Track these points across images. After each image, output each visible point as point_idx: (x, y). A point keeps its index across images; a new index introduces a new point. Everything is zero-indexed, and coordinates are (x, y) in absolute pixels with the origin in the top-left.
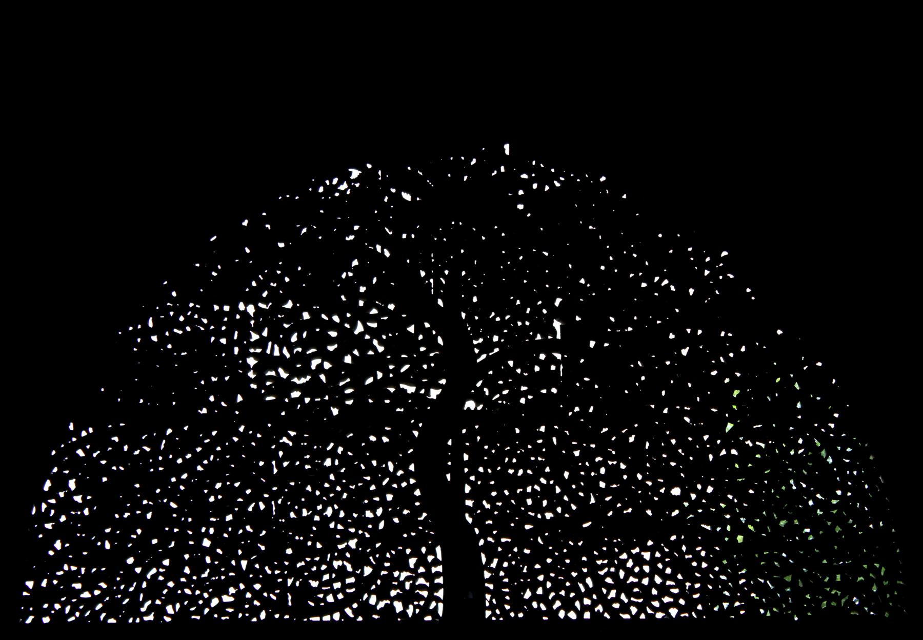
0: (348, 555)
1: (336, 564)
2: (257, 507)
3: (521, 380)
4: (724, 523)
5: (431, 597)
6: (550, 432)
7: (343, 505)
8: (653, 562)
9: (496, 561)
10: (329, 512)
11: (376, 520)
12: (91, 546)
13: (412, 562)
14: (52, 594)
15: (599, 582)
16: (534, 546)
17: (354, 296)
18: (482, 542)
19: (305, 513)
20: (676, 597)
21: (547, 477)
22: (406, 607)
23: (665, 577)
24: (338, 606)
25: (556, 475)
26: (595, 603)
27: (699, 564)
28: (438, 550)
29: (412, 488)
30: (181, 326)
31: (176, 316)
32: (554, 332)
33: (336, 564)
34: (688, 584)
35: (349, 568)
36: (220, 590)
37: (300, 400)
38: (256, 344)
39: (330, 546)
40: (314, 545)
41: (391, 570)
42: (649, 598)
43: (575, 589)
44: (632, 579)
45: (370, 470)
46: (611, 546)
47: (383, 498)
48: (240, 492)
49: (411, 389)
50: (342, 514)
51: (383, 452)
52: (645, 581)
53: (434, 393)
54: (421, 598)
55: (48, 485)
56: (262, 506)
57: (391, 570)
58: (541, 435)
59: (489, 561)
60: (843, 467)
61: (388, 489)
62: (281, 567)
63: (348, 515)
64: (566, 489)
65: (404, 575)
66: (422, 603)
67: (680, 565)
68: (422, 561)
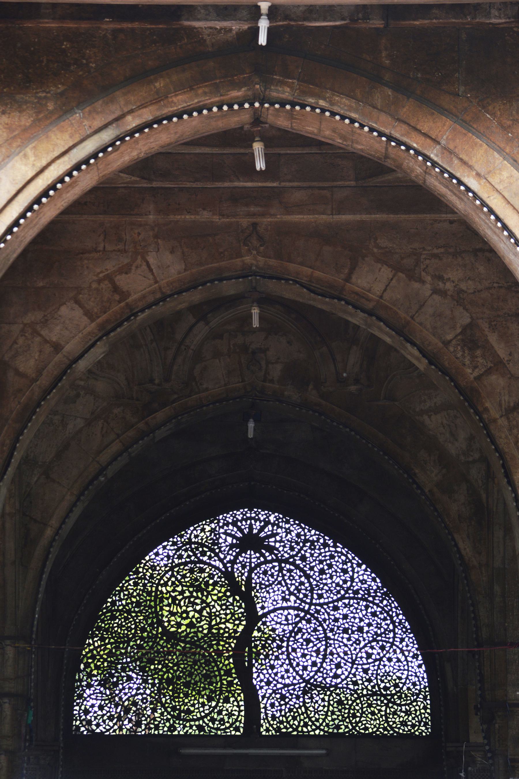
0: (205, 697)
1: (201, 700)
2: (168, 676)
3: (277, 623)
4: (358, 685)
5: (239, 715)
6: (288, 646)
8: (329, 701)
9: (266, 699)
10: (197, 679)
13: (232, 699)
15: (307, 709)
16: (281, 694)
17: (207, 584)
18: (260, 692)
19: (188, 679)
20: (338, 716)
21: (287, 665)
22: (229, 718)
23: (334, 707)
24: (202, 718)
25: (291, 664)
26: (305, 718)
27: (348, 703)
28: (242, 695)
29: (231, 669)
30: (135, 597)
31: (133, 593)
32: (290, 601)
33: (201, 700)
34: (343, 710)
35: (206, 703)
37: (186, 630)
38: (166, 606)
39: (199, 693)
40: (192, 692)
41: (223, 703)
42: (327, 715)
43: (298, 712)
44: (321, 708)
46: (312, 695)
47: (220, 673)
48: (161, 670)
49: (230, 626)
50: (203, 680)
53: (241, 628)
54: (234, 715)
55: (82, 666)
56: (170, 676)
57: (223, 703)
58: (284, 647)
59: (263, 700)
60: (408, 661)
61: (221, 669)
62: (179, 702)
63: (205, 680)
65: (229, 705)
66: (235, 717)
68: (236, 700)
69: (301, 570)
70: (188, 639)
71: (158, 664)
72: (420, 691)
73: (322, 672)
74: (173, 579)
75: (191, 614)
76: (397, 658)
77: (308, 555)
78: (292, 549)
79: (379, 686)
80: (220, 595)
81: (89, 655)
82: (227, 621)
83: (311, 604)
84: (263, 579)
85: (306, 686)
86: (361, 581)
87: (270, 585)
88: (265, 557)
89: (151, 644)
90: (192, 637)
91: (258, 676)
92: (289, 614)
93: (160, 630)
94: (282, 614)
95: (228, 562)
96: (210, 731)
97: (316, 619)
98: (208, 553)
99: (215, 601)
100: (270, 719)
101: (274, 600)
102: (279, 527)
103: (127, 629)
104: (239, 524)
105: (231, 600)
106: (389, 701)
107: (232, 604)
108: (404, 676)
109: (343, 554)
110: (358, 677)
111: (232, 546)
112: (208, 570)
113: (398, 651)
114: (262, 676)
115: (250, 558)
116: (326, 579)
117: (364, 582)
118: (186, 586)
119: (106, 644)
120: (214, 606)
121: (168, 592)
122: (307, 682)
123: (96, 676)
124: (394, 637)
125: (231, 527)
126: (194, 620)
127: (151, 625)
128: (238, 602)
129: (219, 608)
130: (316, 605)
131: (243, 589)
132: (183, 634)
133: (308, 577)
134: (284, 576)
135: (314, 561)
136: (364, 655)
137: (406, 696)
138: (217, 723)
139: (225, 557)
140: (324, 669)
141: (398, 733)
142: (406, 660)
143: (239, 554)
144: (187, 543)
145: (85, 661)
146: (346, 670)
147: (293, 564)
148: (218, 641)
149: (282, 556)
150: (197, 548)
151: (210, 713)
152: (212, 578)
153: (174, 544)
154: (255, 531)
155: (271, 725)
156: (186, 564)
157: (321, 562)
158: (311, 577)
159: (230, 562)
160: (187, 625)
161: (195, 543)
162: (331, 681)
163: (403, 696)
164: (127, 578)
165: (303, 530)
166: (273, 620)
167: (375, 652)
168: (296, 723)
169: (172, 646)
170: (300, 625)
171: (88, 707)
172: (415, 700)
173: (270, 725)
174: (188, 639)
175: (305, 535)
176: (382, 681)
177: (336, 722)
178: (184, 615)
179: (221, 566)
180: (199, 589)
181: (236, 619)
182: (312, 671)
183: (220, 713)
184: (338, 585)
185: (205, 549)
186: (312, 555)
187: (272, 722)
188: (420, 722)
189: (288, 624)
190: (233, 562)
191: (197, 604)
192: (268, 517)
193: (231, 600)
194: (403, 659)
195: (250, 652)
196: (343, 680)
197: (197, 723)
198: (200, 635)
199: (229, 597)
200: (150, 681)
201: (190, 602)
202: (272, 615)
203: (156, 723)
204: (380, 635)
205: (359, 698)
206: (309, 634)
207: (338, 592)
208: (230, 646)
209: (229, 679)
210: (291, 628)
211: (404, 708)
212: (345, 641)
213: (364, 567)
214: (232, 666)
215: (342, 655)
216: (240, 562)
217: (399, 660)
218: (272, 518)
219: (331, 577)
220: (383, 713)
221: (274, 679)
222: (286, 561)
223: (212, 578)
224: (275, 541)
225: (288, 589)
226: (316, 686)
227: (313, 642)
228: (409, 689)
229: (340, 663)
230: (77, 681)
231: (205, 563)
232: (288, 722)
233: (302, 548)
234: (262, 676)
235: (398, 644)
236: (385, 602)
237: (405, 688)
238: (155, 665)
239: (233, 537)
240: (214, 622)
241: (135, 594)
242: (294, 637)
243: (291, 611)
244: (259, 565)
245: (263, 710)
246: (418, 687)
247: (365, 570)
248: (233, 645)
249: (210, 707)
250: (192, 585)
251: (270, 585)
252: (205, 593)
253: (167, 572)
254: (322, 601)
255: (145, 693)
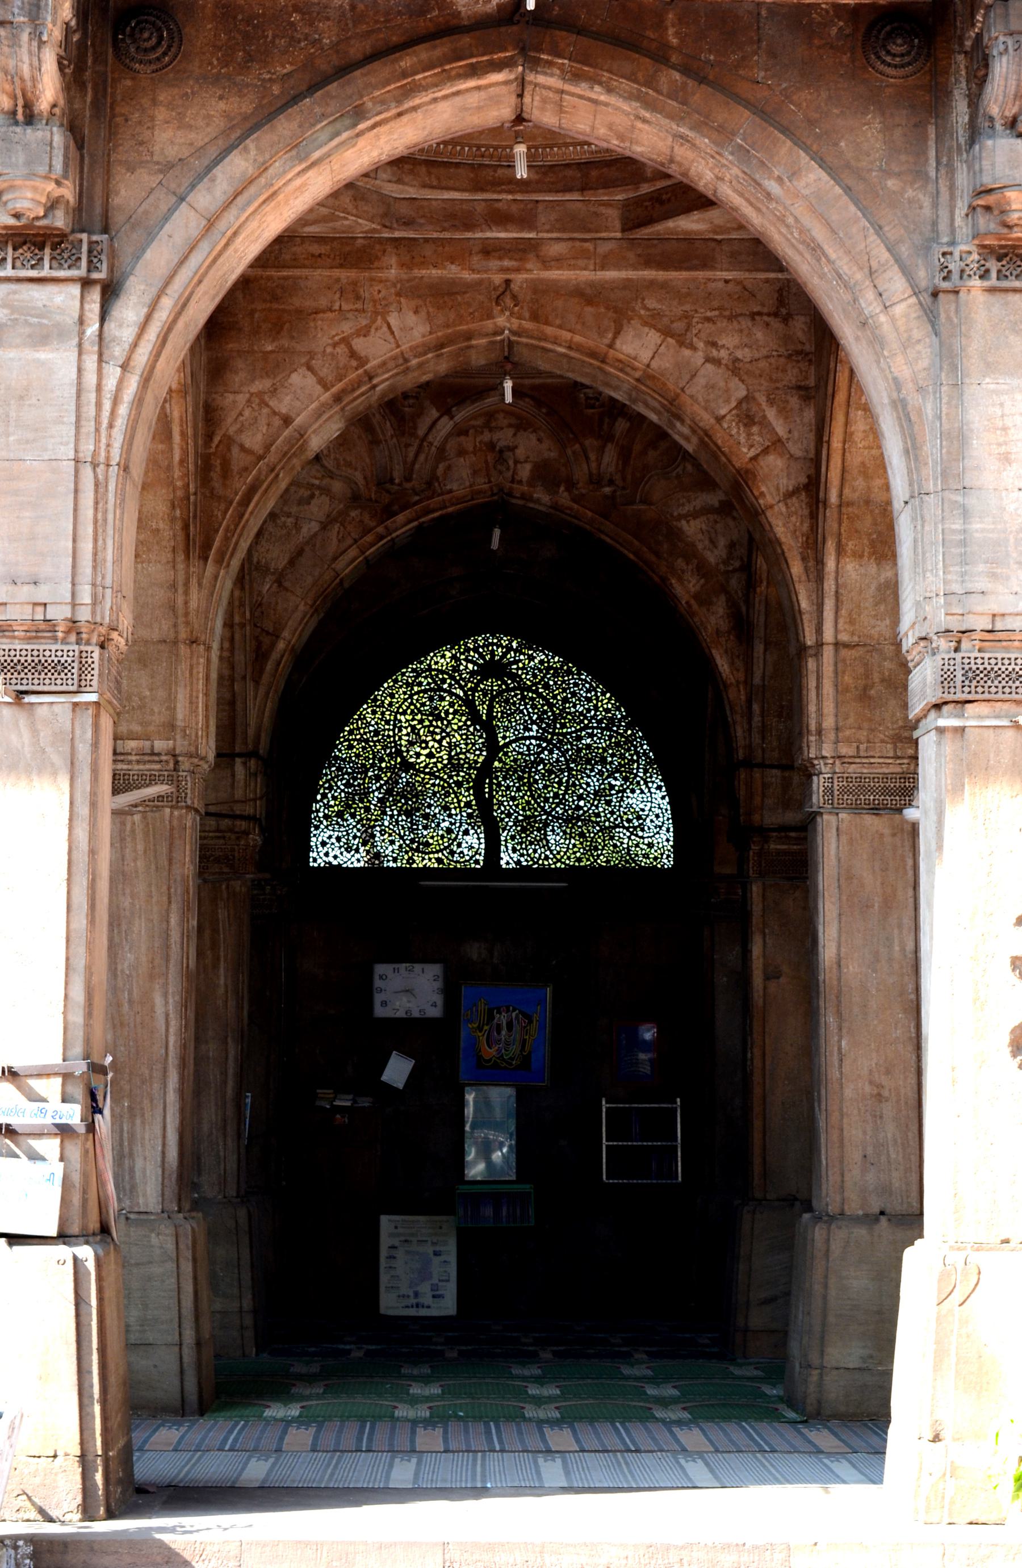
3: (519, 753)
6: (530, 776)
7: (443, 807)
10: (437, 811)
11: (456, 815)
12: (338, 823)
13: (472, 832)
14: (324, 844)
15: (548, 841)
17: (447, 713)
19: (428, 811)
24: (441, 851)
25: (532, 796)
29: (471, 801)
36: (392, 842)
45: (455, 793)
49: (472, 757)
51: (459, 784)
52: (567, 842)
55: (319, 797)
64: (536, 802)
67: (582, 835)
68: (476, 832)
69: (544, 698)
70: (427, 770)
71: (396, 795)
72: (663, 823)
73: (564, 805)
74: (412, 707)
75: (431, 744)
76: (641, 789)
77: (551, 683)
78: (535, 676)
79: (622, 818)
80: (461, 724)
81: (327, 785)
82: (468, 751)
83: (553, 734)
84: (505, 708)
85: (547, 819)
86: (604, 710)
87: (512, 714)
88: (507, 685)
89: (389, 774)
90: (431, 768)
91: (499, 808)
92: (531, 744)
93: (399, 760)
94: (524, 744)
95: (469, 690)
96: (449, 864)
97: (559, 749)
98: (448, 681)
99: (455, 731)
100: (510, 852)
101: (516, 730)
102: (521, 653)
103: (365, 759)
104: (481, 650)
105: (471, 729)
106: (632, 833)
107: (473, 734)
108: (647, 809)
109: (587, 682)
110: (601, 809)
111: (472, 673)
112: (448, 698)
113: (642, 782)
114: (503, 808)
115: (492, 686)
116: (569, 708)
117: (607, 711)
118: (425, 715)
119: (343, 775)
120: (454, 736)
121: (407, 721)
122: (549, 814)
123: (332, 807)
124: (638, 768)
125: (472, 653)
126: (433, 750)
127: (390, 755)
128: (478, 731)
129: (459, 738)
130: (558, 734)
131: (484, 718)
132: (422, 765)
133: (551, 706)
134: (526, 704)
135: (557, 689)
136: (607, 786)
137: (649, 828)
138: (456, 855)
139: (466, 685)
140: (567, 800)
141: (640, 865)
142: (649, 791)
143: (480, 682)
144: (427, 670)
145: (322, 791)
146: (589, 802)
147: (536, 692)
148: (458, 772)
149: (525, 683)
150: (437, 675)
151: (449, 845)
152: (453, 707)
153: (413, 670)
154: (497, 658)
155: (512, 858)
156: (425, 691)
157: (564, 690)
158: (554, 705)
159: (470, 689)
160: (427, 756)
161: (435, 670)
162: (573, 813)
163: (646, 828)
164: (365, 706)
165: (547, 656)
166: (514, 750)
167: (618, 783)
168: (537, 855)
169: (411, 777)
170: (542, 756)
171: (325, 839)
172: (658, 833)
173: (512, 858)
174: (427, 770)
175: (548, 662)
176: (625, 813)
177: (578, 855)
178: (423, 745)
179: (462, 694)
180: (438, 718)
181: (477, 749)
182: (552, 803)
183: (459, 845)
184: (581, 713)
185: (446, 676)
186: (555, 683)
187: (512, 855)
188: (662, 855)
189: (529, 755)
190: (474, 690)
191: (437, 734)
192: (510, 643)
193: (471, 729)
194: (646, 791)
195: (491, 784)
196: (585, 812)
197: (436, 856)
198: (440, 766)
199: (470, 726)
200: (389, 813)
201: (429, 731)
202: (514, 745)
203: (395, 855)
204: (624, 766)
205: (601, 830)
206: (551, 764)
207: (582, 722)
208: (470, 777)
209: (470, 811)
210: (532, 758)
211: (646, 841)
212: (588, 772)
213: (608, 695)
214: (472, 798)
215: (584, 786)
216: (482, 690)
217: (642, 792)
218: (514, 644)
219: (575, 706)
220: (625, 846)
221: (515, 811)
222: (529, 689)
223: (453, 707)
224: (518, 669)
225: (530, 718)
226: (558, 818)
227: (555, 773)
228: (652, 821)
229: (582, 794)
230: (313, 812)
231: (445, 691)
232: (529, 855)
233: (545, 676)
234: (503, 808)
235: (641, 775)
236: (629, 732)
237: (648, 820)
238: (393, 796)
239: (474, 663)
240: (453, 753)
241: (373, 723)
242: (536, 768)
243: (533, 742)
244: (500, 693)
245: (503, 843)
246: (661, 819)
247: (610, 699)
248: (473, 776)
249: (449, 839)
250: (431, 714)
251: (512, 714)
252: (445, 722)
253: (405, 700)
254: (565, 731)
255: (383, 825)
